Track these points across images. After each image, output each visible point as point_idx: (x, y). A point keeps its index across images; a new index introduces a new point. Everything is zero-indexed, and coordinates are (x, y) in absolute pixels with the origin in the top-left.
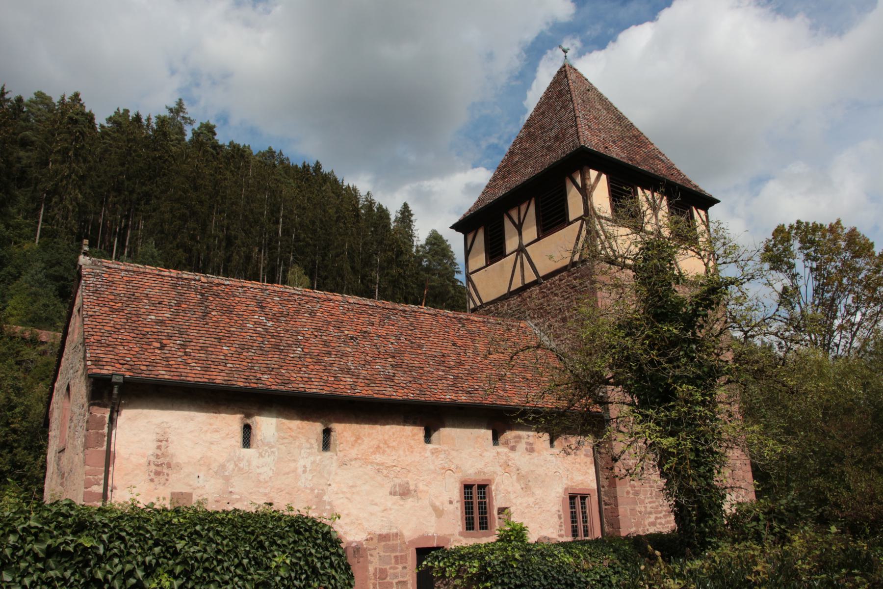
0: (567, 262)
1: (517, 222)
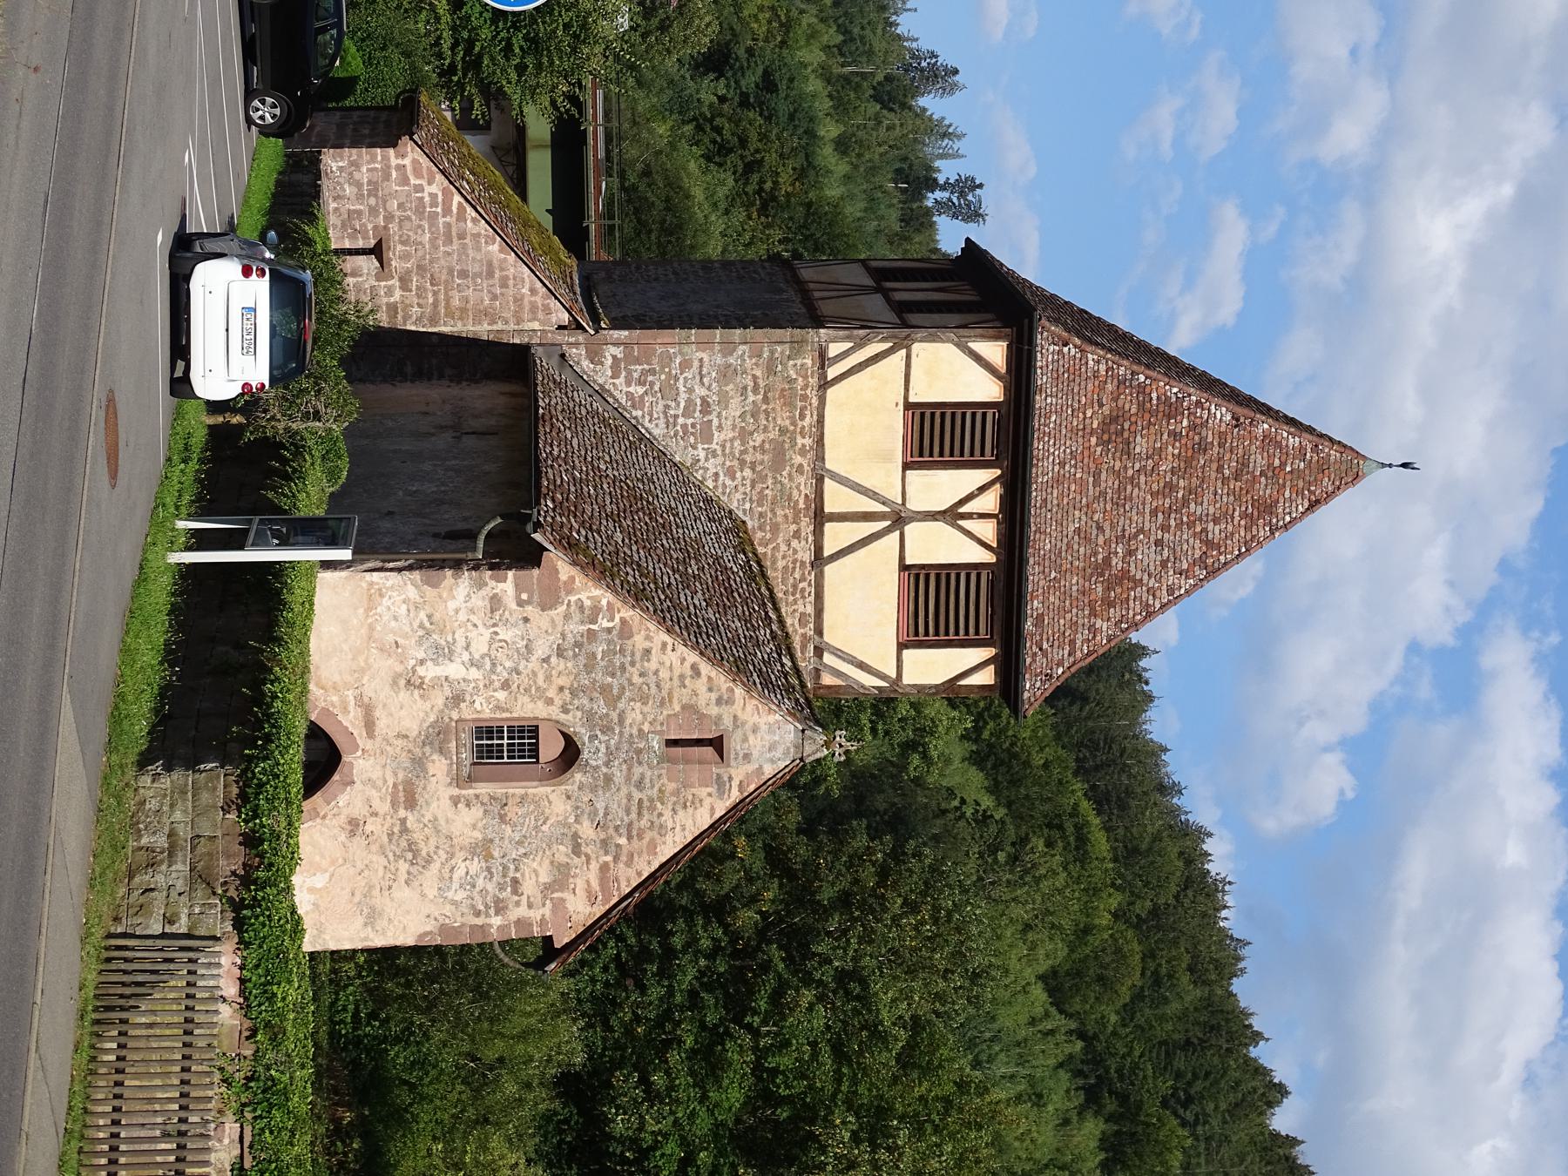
0: (828, 637)
1: (961, 510)
